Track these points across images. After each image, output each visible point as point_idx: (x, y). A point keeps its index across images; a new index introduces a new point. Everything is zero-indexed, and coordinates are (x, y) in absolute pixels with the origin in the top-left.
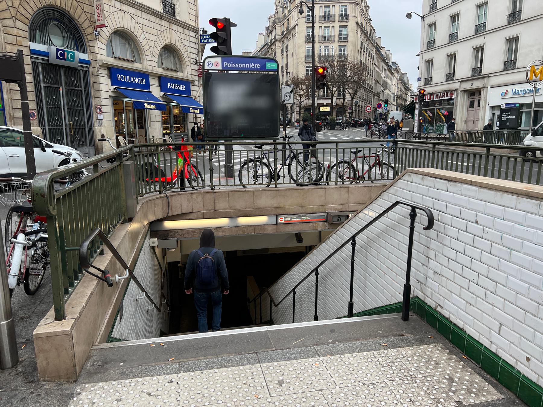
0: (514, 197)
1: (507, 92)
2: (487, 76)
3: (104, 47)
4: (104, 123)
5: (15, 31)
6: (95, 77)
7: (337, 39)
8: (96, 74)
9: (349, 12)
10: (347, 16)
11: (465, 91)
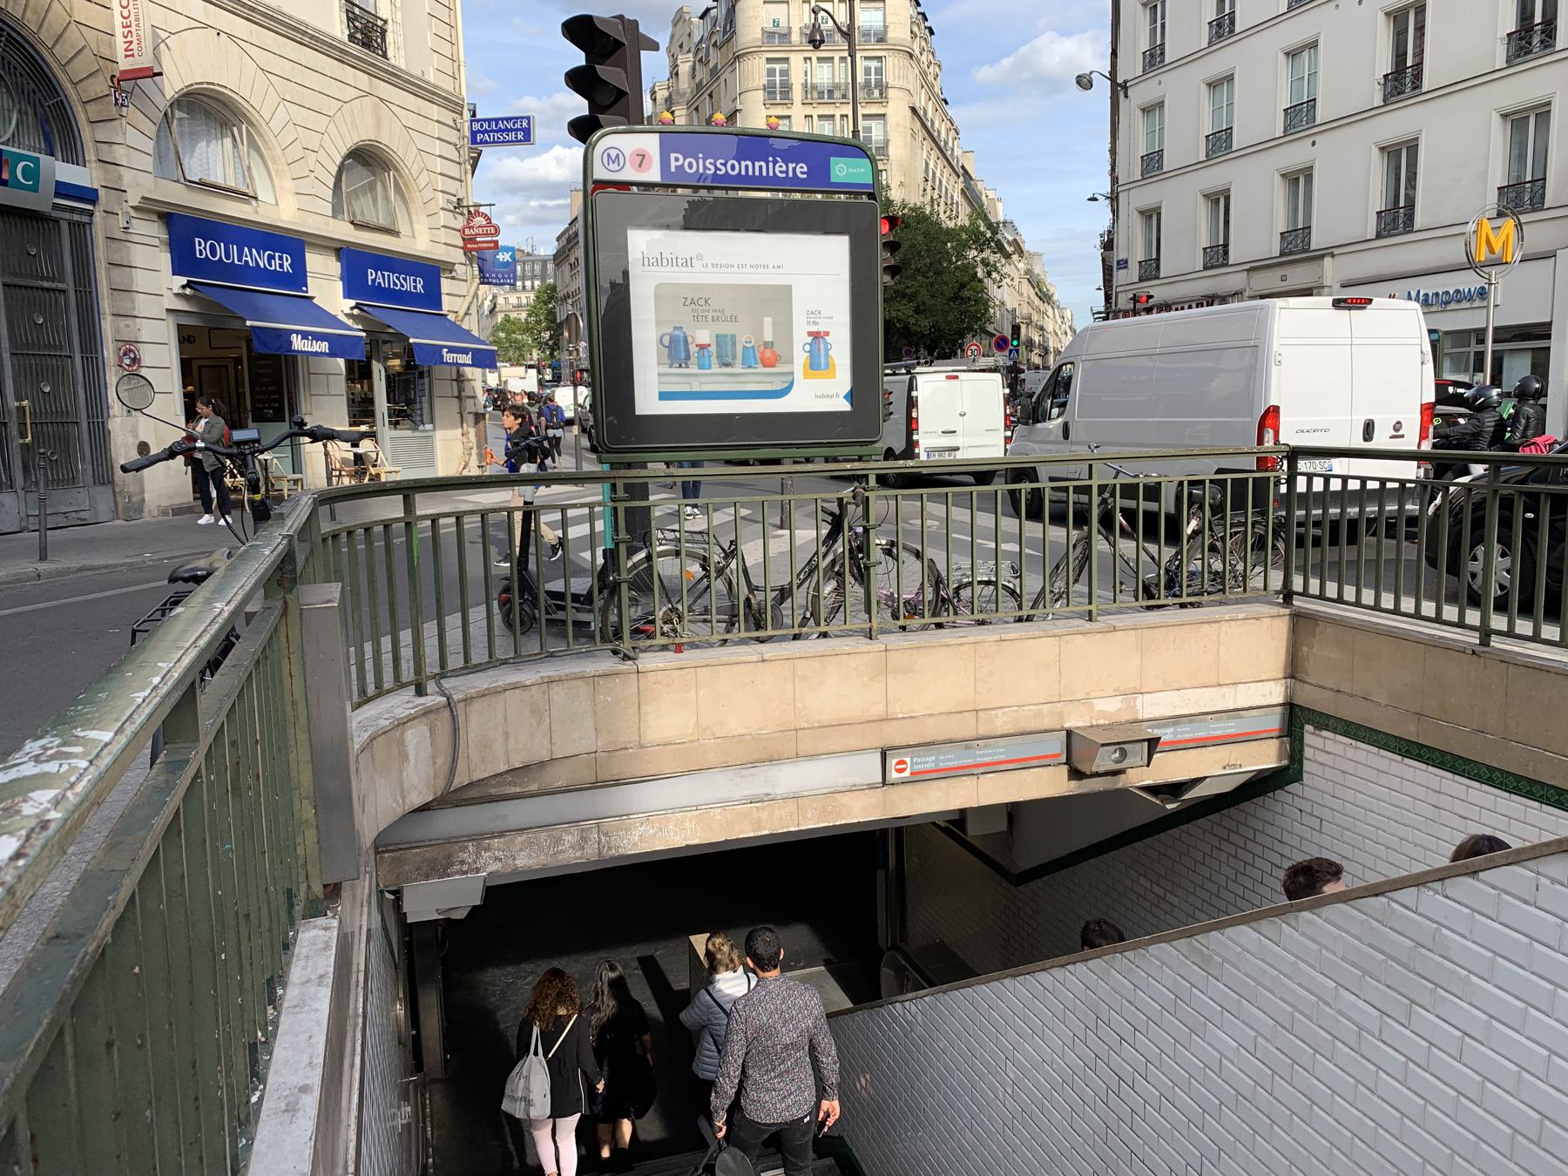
2: (1329, 252)
3: (149, 146)
6: (115, 245)
8: (118, 235)
9: (890, 77)
10: (883, 88)
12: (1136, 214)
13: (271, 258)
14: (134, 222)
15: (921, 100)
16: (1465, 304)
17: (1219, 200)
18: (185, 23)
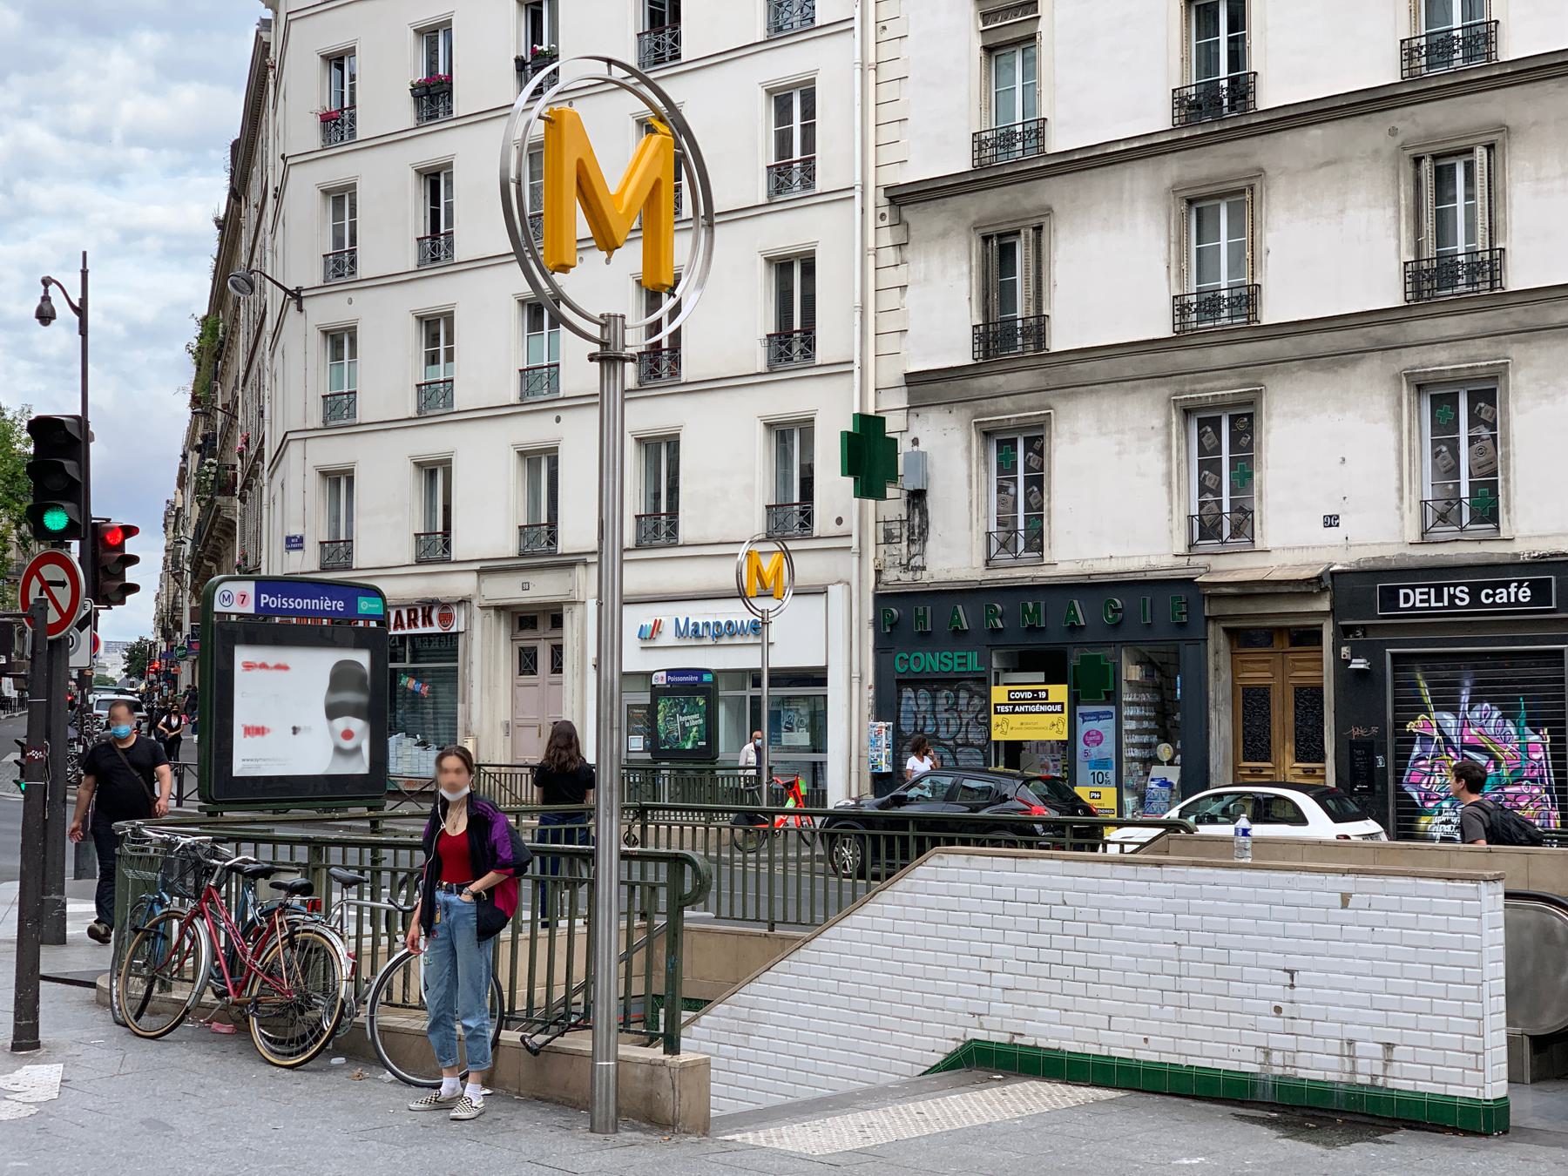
0: (1109, 866)
1: (657, 625)
11: (499, 609)
12: (314, 477)
16: (738, 640)
17: (435, 472)
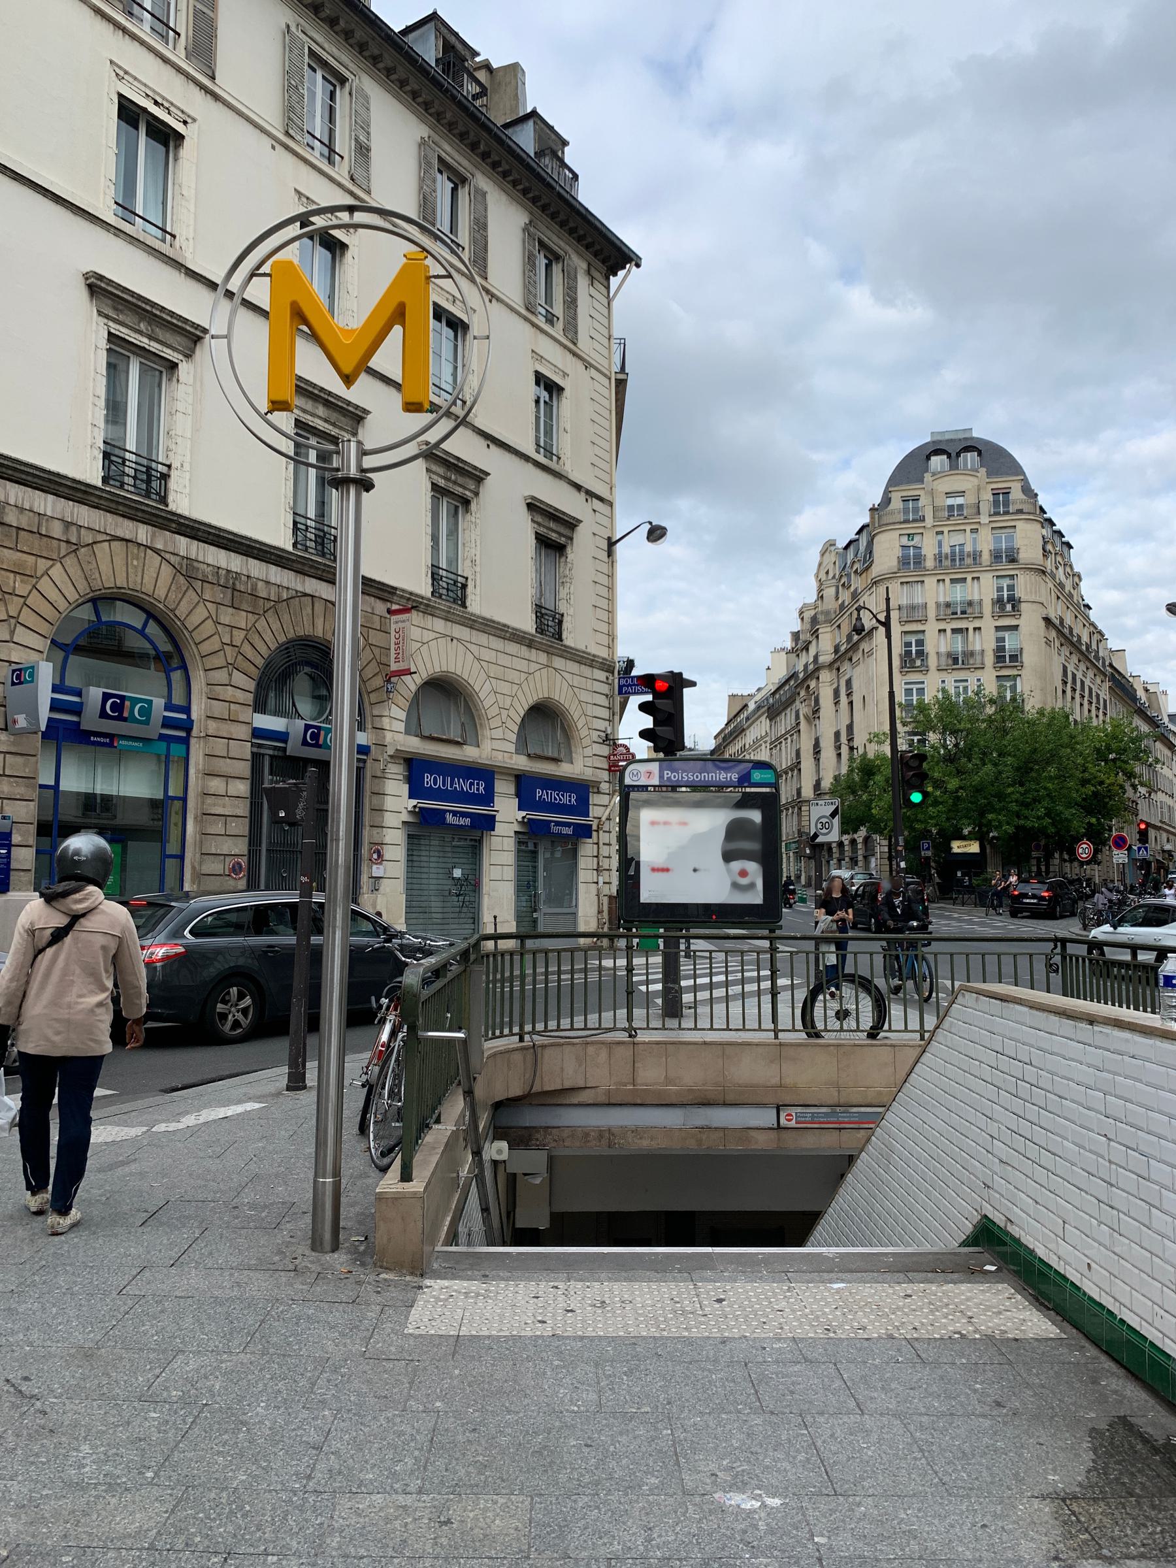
3: (402, 715)
4: (385, 885)
5: (229, 693)
6: (377, 780)
7: (989, 659)
8: (379, 774)
9: (1020, 593)
10: (1015, 602)
13: (471, 784)
14: (390, 765)
15: (1056, 610)
18: (435, 635)
